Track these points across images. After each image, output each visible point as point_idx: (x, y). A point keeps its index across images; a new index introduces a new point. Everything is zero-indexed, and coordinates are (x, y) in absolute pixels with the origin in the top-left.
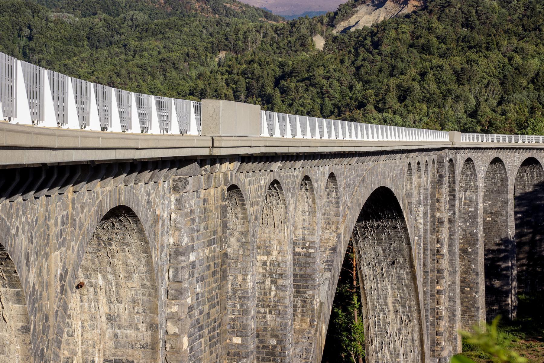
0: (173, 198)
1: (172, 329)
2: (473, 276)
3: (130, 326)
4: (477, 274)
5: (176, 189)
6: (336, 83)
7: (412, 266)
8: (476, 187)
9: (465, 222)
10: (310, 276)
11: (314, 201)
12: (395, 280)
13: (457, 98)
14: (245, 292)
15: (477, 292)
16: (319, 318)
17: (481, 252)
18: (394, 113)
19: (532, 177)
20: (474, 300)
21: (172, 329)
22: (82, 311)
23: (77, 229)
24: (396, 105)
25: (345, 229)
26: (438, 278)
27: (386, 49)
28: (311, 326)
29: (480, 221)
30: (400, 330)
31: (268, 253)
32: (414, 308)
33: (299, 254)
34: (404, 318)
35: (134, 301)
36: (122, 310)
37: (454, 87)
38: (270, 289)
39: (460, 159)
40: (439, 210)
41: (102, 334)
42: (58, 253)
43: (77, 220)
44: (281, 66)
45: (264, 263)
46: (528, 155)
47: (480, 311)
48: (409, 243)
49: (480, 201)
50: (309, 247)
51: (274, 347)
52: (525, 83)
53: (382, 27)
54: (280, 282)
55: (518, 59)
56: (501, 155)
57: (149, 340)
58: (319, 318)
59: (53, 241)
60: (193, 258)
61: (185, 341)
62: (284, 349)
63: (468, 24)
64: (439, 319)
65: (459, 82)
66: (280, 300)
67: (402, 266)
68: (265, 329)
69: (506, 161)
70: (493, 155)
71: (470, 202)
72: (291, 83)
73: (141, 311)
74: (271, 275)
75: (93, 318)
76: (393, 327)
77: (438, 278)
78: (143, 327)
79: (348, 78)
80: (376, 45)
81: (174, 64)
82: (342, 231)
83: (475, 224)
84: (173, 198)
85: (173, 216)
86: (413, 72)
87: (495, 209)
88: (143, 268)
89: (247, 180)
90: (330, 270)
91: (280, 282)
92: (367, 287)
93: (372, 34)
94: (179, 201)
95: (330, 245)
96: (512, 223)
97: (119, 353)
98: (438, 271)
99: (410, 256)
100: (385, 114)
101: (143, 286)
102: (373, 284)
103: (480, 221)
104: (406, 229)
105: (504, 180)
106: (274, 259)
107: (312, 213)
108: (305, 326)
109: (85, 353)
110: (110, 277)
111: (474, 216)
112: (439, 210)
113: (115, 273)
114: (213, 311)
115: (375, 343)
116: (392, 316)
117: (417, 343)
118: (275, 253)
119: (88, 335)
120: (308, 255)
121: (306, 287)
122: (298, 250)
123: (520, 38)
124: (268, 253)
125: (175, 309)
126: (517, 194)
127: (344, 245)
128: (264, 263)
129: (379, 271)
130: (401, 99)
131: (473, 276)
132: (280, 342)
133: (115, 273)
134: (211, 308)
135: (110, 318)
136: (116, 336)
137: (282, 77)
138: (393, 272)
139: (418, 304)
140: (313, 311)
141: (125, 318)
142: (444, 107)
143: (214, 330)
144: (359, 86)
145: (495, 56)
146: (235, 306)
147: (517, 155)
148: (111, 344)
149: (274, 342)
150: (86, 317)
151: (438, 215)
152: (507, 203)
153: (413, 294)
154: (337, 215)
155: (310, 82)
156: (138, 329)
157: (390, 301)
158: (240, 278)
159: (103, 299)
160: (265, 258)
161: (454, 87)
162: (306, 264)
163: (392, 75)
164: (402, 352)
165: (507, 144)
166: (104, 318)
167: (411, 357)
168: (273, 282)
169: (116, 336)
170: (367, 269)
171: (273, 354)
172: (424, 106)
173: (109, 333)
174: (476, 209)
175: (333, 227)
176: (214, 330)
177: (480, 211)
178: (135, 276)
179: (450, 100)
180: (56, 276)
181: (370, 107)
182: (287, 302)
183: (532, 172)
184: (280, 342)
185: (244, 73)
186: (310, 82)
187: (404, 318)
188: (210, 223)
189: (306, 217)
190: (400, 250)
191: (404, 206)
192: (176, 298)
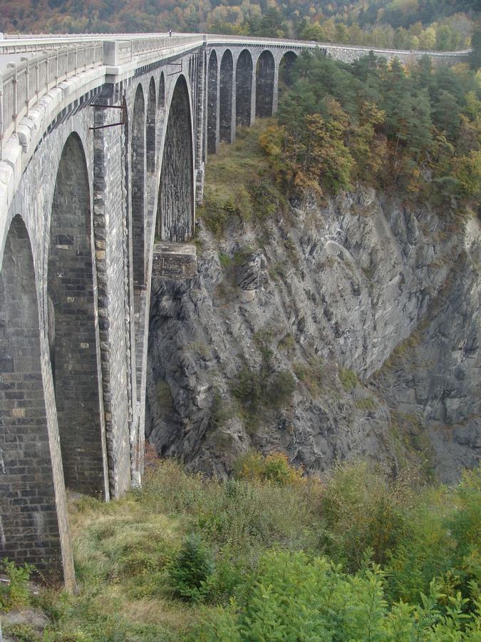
3: (70, 212)
4: (216, 119)
15: (215, 129)
29: (218, 87)
35: (72, 194)
46: (244, 48)
49: (219, 74)
57: (84, 221)
59: (39, 182)
69: (232, 52)
73: (77, 201)
97: (61, 230)
101: (79, 184)
103: (218, 87)
106: (135, 135)
117: (189, 164)
156: (75, 214)
157: (175, 140)
174: (216, 80)
177: (218, 82)
178: (74, 177)
187: (183, 150)
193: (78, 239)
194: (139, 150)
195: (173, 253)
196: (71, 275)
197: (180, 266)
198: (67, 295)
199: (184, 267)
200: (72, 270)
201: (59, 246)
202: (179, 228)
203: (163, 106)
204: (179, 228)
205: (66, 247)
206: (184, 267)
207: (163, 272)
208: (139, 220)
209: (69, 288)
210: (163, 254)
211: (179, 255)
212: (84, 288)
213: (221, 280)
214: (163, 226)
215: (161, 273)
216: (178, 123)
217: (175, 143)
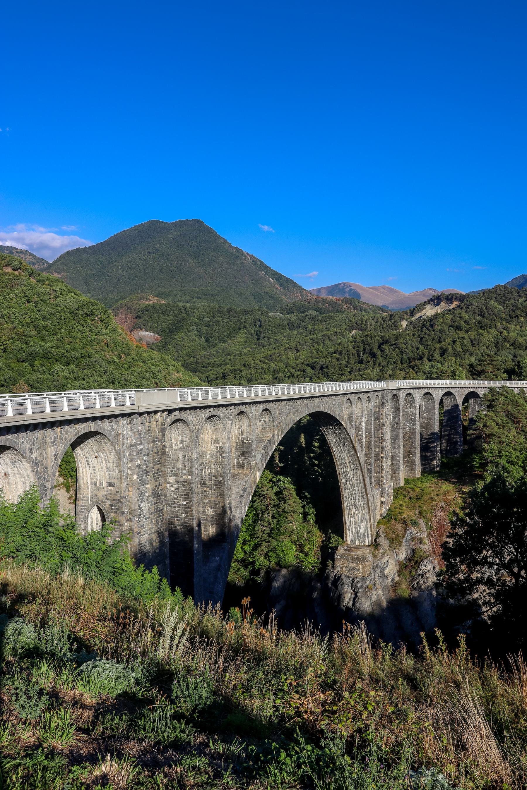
0: (129, 426)
1: (130, 472)
2: (414, 450)
3: (113, 471)
4: (415, 448)
5: (130, 423)
6: (410, 347)
7: (353, 446)
8: (415, 407)
9: (410, 423)
10: (250, 452)
11: (250, 421)
12: (347, 452)
13: (472, 354)
14: (192, 459)
16: (254, 469)
17: (418, 438)
18: (438, 362)
19: (451, 401)
20: (414, 461)
21: (130, 472)
22: (98, 466)
24: (439, 358)
25: (278, 432)
26: (382, 451)
27: (437, 328)
28: (250, 473)
30: (353, 475)
31: (218, 443)
32: (358, 465)
34: (355, 470)
35: (113, 462)
36: (110, 465)
37: (470, 348)
39: (402, 395)
40: (382, 419)
41: (105, 473)
42: (53, 448)
44: (382, 337)
45: (217, 447)
46: (447, 390)
47: (417, 466)
48: (349, 435)
50: (249, 440)
51: (221, 481)
52: (508, 346)
53: (437, 316)
54: (223, 455)
55: (505, 333)
56: (430, 391)
58: (254, 469)
60: (140, 447)
61: (135, 477)
62: (225, 481)
63: (482, 315)
64: (382, 470)
65: (473, 345)
66: (223, 462)
67: (349, 446)
68: (218, 474)
70: (426, 391)
71: (412, 414)
72: (386, 347)
75: (102, 468)
76: (350, 474)
77: (382, 451)
78: (117, 471)
79: (416, 343)
80: (432, 326)
81: (329, 337)
82: (276, 433)
83: (414, 424)
84: (129, 426)
85: (129, 433)
86: (449, 340)
87: (429, 417)
88: (114, 451)
89: (190, 417)
90: (264, 449)
91: (223, 455)
92: (336, 455)
93: (431, 320)
94: (131, 428)
95: (268, 439)
96: (437, 423)
98: (382, 448)
99: (351, 441)
100: (432, 363)
102: (338, 454)
104: (346, 430)
105: (433, 402)
107: (250, 426)
108: (248, 472)
109: (100, 480)
110: (105, 454)
111: (414, 420)
112: (382, 419)
113: (106, 453)
114: (155, 466)
115: (343, 481)
116: (349, 469)
117: (362, 481)
118: (221, 443)
119: (101, 474)
120: (249, 443)
121: (248, 457)
122: (245, 441)
123: (507, 321)
124: (218, 443)
125: (130, 465)
126: (445, 408)
127: (278, 439)
128: (217, 447)
129: (339, 448)
130: (442, 355)
131: (414, 450)
132: (223, 478)
133: (106, 453)
134: (154, 465)
135: (107, 468)
136: (109, 474)
137: (382, 344)
138: (346, 448)
139: (360, 463)
140: (251, 466)
141: (111, 468)
142: (464, 358)
143: (157, 473)
144: (421, 348)
145: (493, 331)
147: (440, 390)
148: (108, 477)
149: (221, 479)
150: (100, 467)
151: (382, 421)
152: (435, 414)
153: (357, 459)
154: (273, 426)
155: (396, 346)
157: (347, 461)
158: (190, 454)
159: (104, 462)
161: (470, 348)
162: (248, 447)
163: (439, 341)
164: (356, 485)
165: (432, 385)
166: (105, 468)
167: (360, 487)
168: (220, 455)
169: (109, 474)
170: (334, 447)
171: (221, 483)
172: (454, 358)
173: (107, 473)
174: (415, 417)
175: (272, 431)
176: (157, 473)
179: (468, 355)
180: (51, 455)
181: (425, 359)
182: (226, 463)
183: (451, 399)
184: (223, 478)
185: (362, 341)
186: (396, 346)
187: (355, 470)
188: (153, 435)
189: (247, 428)
190: (346, 439)
191: (342, 419)
192: (131, 462)
193: (117, 485)
196: (114, 503)
198: (112, 512)
200: (114, 500)
201: (109, 488)
202: (361, 534)
204: (361, 534)
205: (112, 488)
206: (360, 566)
208: (223, 498)
209: (112, 509)
211: (356, 555)
212: (119, 509)
214: (348, 531)
216: (346, 448)
217: (348, 464)
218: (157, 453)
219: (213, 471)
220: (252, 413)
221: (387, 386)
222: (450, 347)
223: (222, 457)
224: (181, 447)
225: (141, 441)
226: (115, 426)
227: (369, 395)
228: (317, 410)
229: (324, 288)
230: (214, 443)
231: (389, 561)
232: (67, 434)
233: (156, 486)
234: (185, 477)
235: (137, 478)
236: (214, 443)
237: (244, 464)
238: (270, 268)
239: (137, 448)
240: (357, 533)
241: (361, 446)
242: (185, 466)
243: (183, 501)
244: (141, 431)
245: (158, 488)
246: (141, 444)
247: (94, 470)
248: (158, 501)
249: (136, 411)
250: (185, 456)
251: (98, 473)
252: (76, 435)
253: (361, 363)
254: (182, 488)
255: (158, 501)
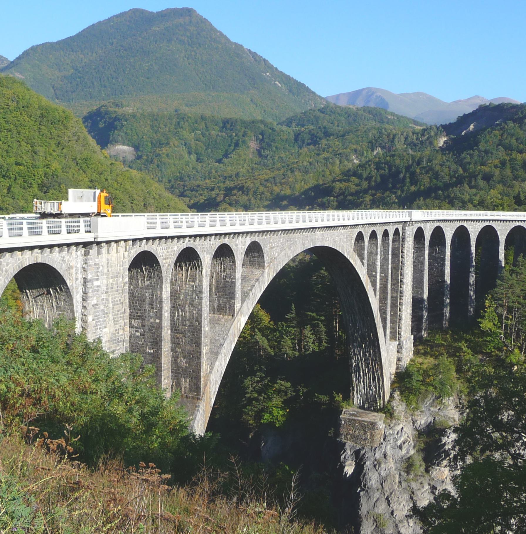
6: (446, 170)
23: (4, 272)
33: (228, 282)
38: (195, 298)
43: (4, 269)
45: (193, 286)
51: (197, 326)
68: (193, 318)
74: (196, 292)
81: (346, 156)
89: (159, 248)
114: (115, 306)
118: (197, 281)
122: (228, 280)
124: (194, 282)
146: (156, 306)
160: (193, 283)
176: (118, 314)
194: (200, 295)
195: (360, 419)
197: (365, 433)
199: (369, 434)
203: (264, 269)
204: (371, 396)
207: (349, 437)
208: (198, 346)
210: (349, 419)
211: (364, 421)
213: (412, 452)
215: (347, 438)
218: (117, 291)
219: (188, 314)
220: (237, 245)
221: (410, 215)
222: (497, 172)
223: (198, 298)
224: (148, 285)
225: (98, 276)
226: (67, 258)
227: (386, 227)
228: (319, 244)
229: (344, 94)
230: (189, 281)
231: (404, 429)
232: (7, 265)
233: (116, 330)
234: (152, 320)
235: (93, 320)
236: (189, 281)
237: (226, 308)
238: (276, 69)
239: (93, 284)
240: (367, 395)
241: (375, 290)
242: (153, 308)
243: (150, 349)
244: (98, 264)
245: (118, 333)
246: (97, 279)
247: (43, 309)
248: (118, 348)
249: (93, 240)
250: (153, 295)
251: (47, 312)
252: (19, 267)
253: (93, 129)
254: (149, 335)
255: (118, 348)
